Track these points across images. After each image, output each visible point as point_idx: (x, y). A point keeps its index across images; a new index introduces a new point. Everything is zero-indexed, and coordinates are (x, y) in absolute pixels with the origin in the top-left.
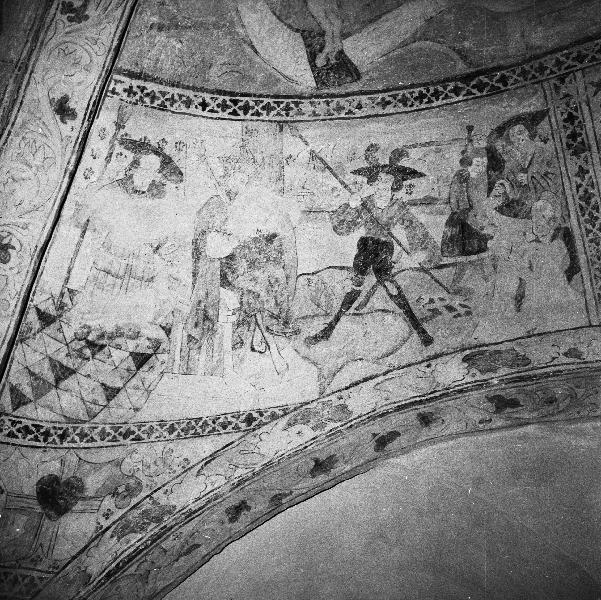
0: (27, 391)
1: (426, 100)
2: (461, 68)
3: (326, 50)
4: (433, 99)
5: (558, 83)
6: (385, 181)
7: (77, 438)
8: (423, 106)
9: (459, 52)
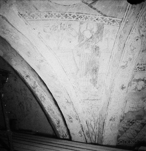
7: (132, 142)
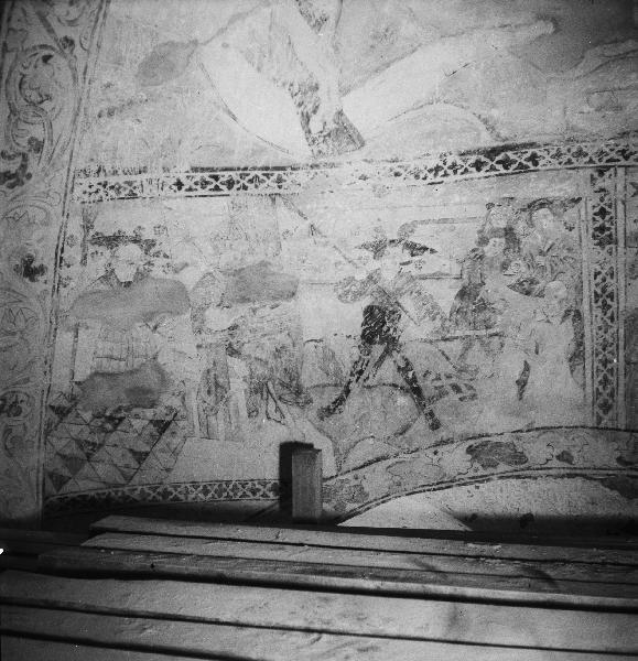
0: (66, 472)
1: (441, 173)
2: (487, 141)
3: (320, 112)
4: (450, 172)
5: (596, 175)
6: (397, 254)
8: (438, 179)
9: (485, 122)
